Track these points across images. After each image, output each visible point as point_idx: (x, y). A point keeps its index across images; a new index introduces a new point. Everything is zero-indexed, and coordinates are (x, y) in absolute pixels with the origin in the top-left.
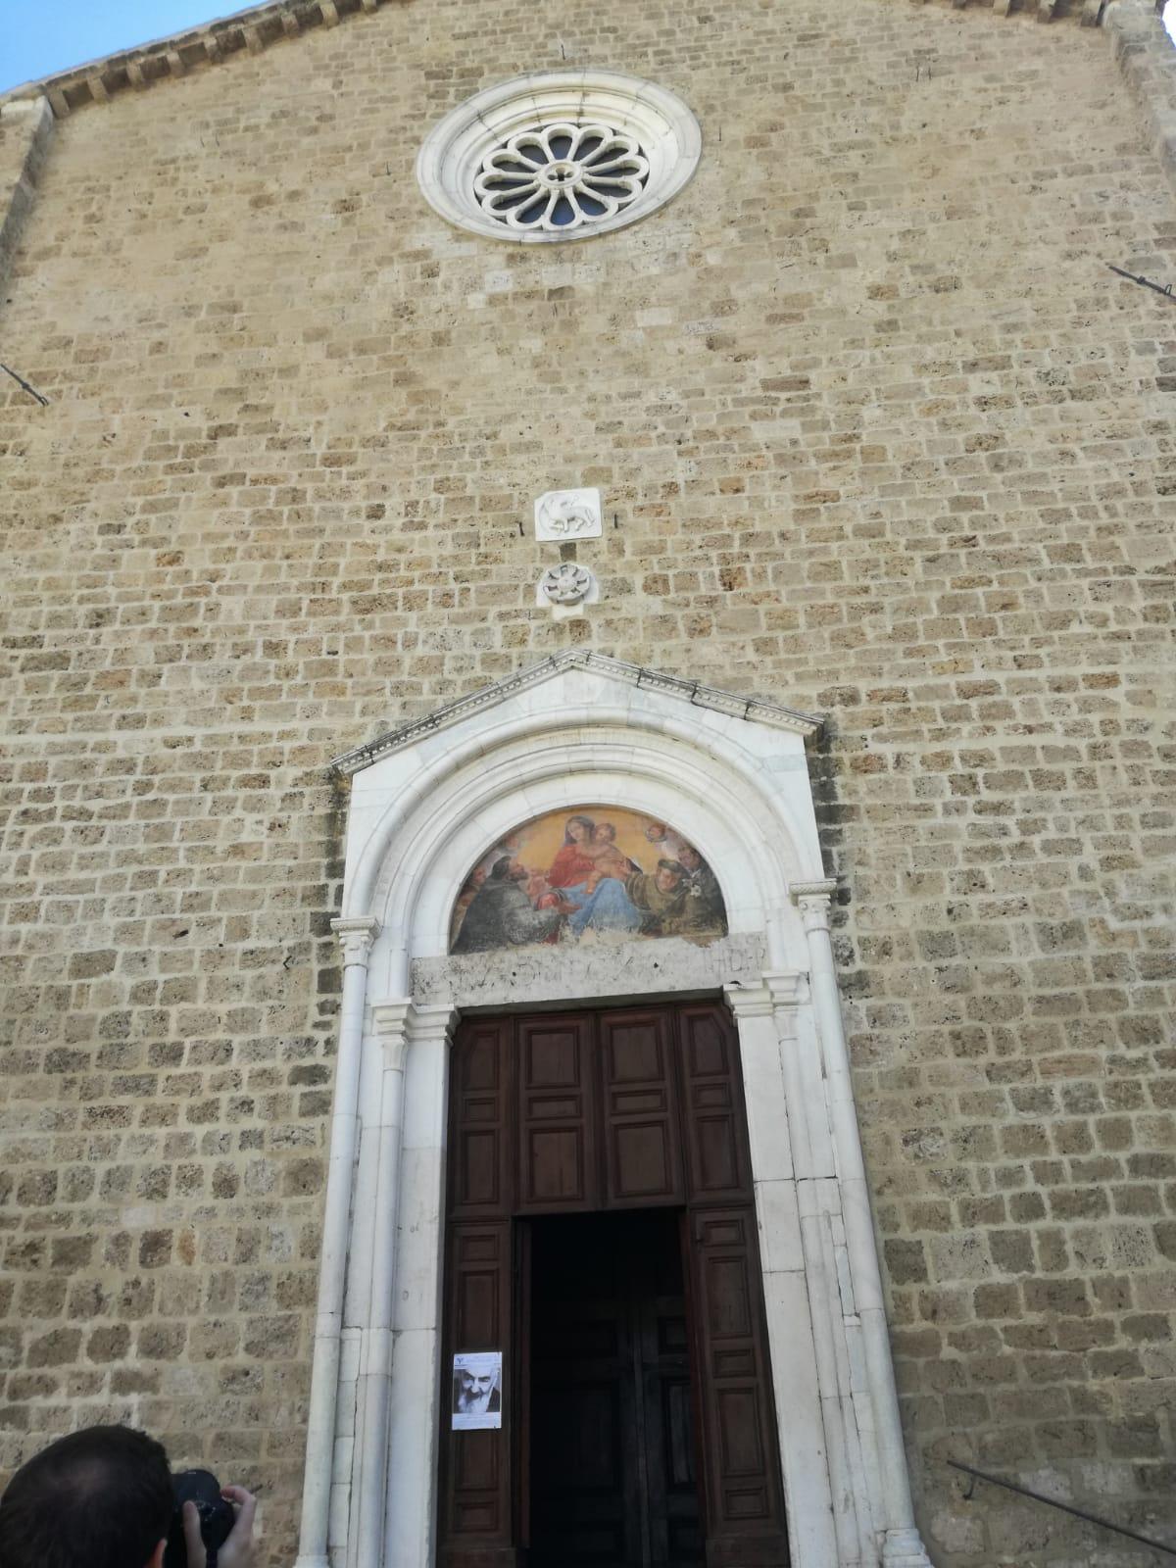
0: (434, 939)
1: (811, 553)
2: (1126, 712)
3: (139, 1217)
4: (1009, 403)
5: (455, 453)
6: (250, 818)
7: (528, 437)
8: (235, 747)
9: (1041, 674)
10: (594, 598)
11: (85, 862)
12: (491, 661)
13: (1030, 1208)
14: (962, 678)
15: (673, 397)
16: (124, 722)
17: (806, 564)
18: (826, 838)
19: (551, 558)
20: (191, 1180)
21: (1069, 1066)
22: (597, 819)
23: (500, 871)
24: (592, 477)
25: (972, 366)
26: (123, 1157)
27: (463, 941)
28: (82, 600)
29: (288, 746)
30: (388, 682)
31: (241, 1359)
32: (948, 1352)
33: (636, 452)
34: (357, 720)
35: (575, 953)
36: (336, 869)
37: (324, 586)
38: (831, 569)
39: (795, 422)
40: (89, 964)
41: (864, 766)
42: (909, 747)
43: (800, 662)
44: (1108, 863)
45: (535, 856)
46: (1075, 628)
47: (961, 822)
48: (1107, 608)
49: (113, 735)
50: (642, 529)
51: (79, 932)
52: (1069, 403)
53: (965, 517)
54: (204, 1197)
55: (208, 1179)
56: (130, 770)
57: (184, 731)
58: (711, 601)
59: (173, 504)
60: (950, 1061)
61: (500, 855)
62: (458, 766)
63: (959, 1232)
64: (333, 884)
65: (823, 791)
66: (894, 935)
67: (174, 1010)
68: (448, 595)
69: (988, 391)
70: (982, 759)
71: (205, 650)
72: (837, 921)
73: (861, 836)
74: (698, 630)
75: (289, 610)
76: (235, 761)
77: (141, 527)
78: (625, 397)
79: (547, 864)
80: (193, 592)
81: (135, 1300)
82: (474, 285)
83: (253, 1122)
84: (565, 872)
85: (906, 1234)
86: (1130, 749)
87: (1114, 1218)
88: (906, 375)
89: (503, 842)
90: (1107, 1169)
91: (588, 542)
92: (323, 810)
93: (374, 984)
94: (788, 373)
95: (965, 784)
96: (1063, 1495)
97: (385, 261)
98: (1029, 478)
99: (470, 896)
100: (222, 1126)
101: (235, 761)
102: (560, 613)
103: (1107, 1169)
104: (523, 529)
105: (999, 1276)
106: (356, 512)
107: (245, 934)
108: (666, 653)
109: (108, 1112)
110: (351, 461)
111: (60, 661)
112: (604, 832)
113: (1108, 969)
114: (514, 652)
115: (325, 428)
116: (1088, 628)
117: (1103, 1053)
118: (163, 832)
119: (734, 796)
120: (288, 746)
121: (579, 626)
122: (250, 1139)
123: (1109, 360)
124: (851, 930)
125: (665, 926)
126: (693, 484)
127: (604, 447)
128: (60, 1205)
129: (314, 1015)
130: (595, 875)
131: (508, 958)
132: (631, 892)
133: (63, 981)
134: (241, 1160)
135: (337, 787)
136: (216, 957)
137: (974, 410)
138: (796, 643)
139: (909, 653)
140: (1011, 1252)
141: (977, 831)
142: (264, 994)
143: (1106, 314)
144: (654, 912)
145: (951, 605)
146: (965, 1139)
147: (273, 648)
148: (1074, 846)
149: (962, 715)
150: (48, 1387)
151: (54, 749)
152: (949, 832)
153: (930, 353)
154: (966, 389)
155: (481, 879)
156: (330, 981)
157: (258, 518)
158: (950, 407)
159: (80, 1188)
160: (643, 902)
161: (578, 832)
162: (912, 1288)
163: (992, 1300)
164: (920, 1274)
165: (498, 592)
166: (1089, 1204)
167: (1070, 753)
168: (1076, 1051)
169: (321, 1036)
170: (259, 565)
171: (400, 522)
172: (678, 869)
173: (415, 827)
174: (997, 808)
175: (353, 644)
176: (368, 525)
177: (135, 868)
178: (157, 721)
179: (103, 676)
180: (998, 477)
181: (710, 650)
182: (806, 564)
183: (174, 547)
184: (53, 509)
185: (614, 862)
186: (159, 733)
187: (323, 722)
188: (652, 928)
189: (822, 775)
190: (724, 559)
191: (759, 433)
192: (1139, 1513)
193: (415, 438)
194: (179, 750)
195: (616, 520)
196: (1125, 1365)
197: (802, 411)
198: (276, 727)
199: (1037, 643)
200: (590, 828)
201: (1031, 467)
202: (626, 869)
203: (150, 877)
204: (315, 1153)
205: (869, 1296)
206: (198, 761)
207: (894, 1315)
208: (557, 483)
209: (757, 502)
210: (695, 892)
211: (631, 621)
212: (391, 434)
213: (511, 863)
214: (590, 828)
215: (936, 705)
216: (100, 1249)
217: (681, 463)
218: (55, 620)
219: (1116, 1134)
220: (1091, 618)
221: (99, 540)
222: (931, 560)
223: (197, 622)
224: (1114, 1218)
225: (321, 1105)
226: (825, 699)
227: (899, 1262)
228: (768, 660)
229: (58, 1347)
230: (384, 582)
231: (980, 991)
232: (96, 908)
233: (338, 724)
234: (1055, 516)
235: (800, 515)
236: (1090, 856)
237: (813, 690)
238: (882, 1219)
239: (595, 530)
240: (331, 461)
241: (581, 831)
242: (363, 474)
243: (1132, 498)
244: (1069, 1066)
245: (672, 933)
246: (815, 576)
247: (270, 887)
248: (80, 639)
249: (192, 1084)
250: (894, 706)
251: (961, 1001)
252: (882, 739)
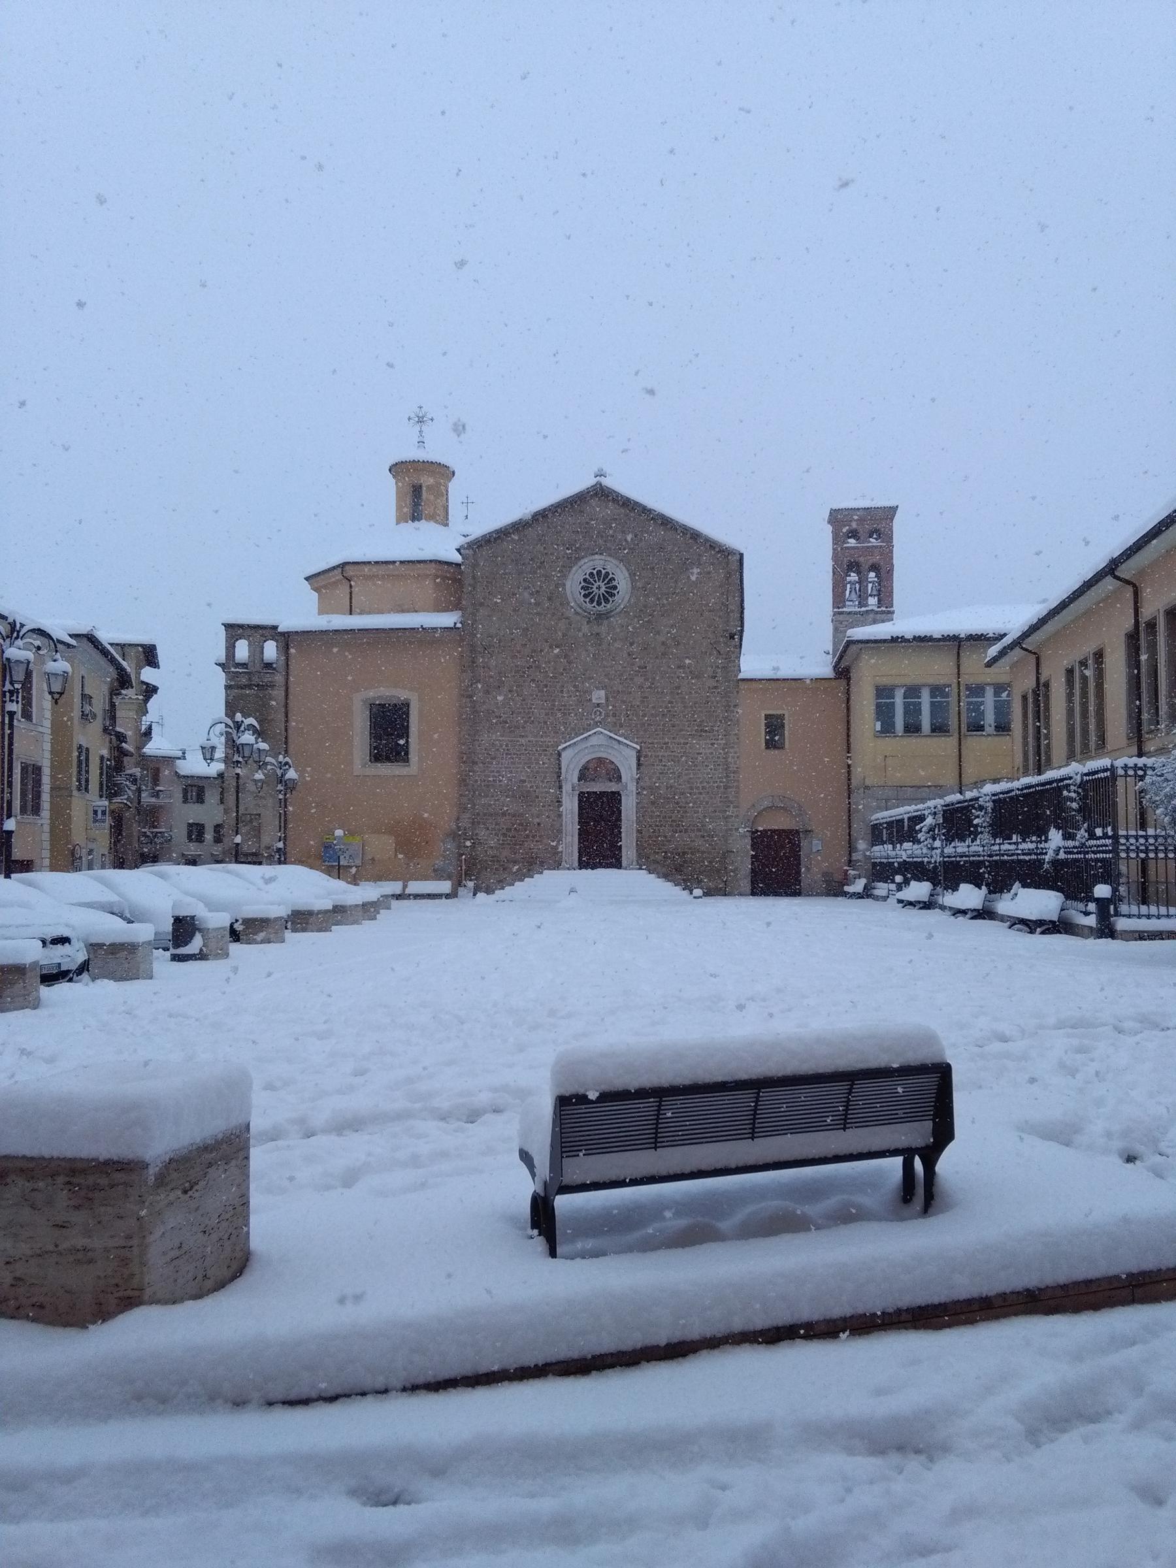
0: (575, 780)
24: (604, 687)
65: (639, 760)
82: (579, 630)
93: (567, 787)
97: (560, 619)
119: (625, 759)
135: (559, 755)
156: (560, 787)
173: (573, 760)
195: (607, 699)
208: (598, 688)
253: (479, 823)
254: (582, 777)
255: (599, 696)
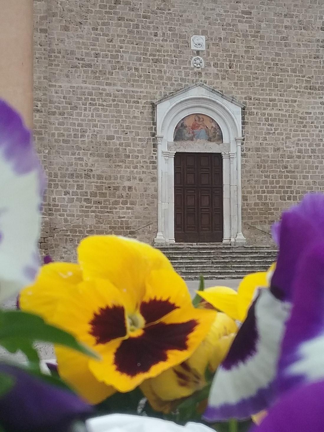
0: (172, 139)
1: (247, 62)
2: (296, 109)
3: (127, 184)
4: (291, 29)
5: (173, 20)
6: (137, 110)
7: (189, 18)
8: (131, 93)
9: (284, 98)
10: (203, 67)
11: (105, 116)
12: (182, 79)
13: (264, 192)
14: (270, 97)
15: (222, 12)
16: (107, 84)
17: (246, 64)
18: (243, 128)
19: (194, 54)
20: (135, 178)
21: (273, 171)
22: (201, 117)
23: (182, 125)
24: (204, 33)
25: (286, 16)
26: (122, 173)
27: (176, 139)
28: (92, 49)
29: (142, 95)
30: (161, 82)
31: (146, 206)
32: (249, 211)
33: (213, 27)
34: (155, 90)
35: (196, 144)
36: (155, 124)
37: (146, 54)
38: (249, 67)
39: (248, 25)
40: (110, 138)
41: (251, 114)
42: (259, 111)
43: (242, 89)
44: (287, 138)
45: (189, 123)
46: (291, 89)
47: (265, 127)
48: (298, 85)
49: (106, 87)
50: (214, 50)
51: (106, 131)
52: (303, 31)
53: (277, 58)
54: (137, 181)
55: (138, 179)
56: (110, 96)
57: (121, 88)
58: (227, 71)
59: (108, 24)
60: (257, 170)
61: (182, 122)
62: (177, 104)
63: (253, 195)
64: (154, 127)
65: (243, 118)
66: (251, 147)
67: (128, 148)
68: (172, 61)
69: (288, 24)
70: (271, 115)
71: (122, 68)
72: (242, 144)
73: (249, 128)
74: (223, 79)
75: (139, 60)
76: (132, 97)
77: (102, 30)
78: (211, 10)
79: (191, 125)
80: (116, 51)
81: (128, 196)
83: (144, 170)
84: (194, 127)
85: (246, 195)
86: (296, 116)
87: (275, 194)
88: (272, 16)
89: (182, 119)
90: (276, 187)
91: (202, 51)
92: (150, 111)
93: (162, 147)
94: (247, 9)
95: (267, 120)
96: (261, 229)
98: (291, 50)
99: (177, 130)
100: (139, 170)
101: (132, 97)
102: (196, 70)
103: (276, 187)
104: (189, 46)
105: (257, 201)
106: (151, 34)
107: (139, 135)
108: (217, 83)
109: (118, 166)
110: (149, 18)
111: (90, 66)
112: (201, 119)
113: (283, 156)
114: (187, 78)
115: (142, 6)
116: (294, 89)
117: (279, 170)
118: (119, 112)
120: (142, 95)
121: (200, 73)
122: (143, 172)
123: (313, 20)
124: (244, 146)
125: (212, 140)
126: (225, 39)
127: (206, 25)
128: (112, 181)
129: (153, 152)
130: (200, 128)
131: (185, 143)
132: (206, 132)
133: (106, 141)
134: (143, 176)
135: (154, 106)
136: (134, 139)
137: (283, 29)
138: (242, 84)
139: (262, 90)
140: (260, 198)
141: (268, 129)
142: (143, 147)
143: (315, 6)
144: (210, 137)
145: (271, 80)
146: (256, 181)
147: (136, 69)
148: (282, 134)
149: (268, 105)
150: (116, 208)
151: (93, 89)
152: (263, 129)
153: (278, 10)
154: (283, 23)
155: (179, 127)
156: (155, 146)
157: (130, 32)
158: (279, 27)
159: (116, 178)
160: (208, 135)
161: (197, 119)
162: (245, 202)
163: (256, 204)
164: (247, 200)
165: (183, 61)
166: (272, 192)
167: (285, 116)
168: (275, 169)
169: (154, 156)
170: (131, 46)
171: (161, 38)
172: (215, 128)
174: (271, 125)
175: (153, 71)
176: (154, 38)
177: (115, 119)
178: (114, 85)
179: (100, 71)
180: (285, 48)
181: (225, 83)
182: (246, 64)
183: (110, 37)
184: (79, 20)
185: (203, 126)
186: (115, 88)
187: (148, 90)
188: (210, 140)
189: (243, 113)
190: (230, 61)
191: (240, 26)
192: (269, 232)
193: (164, 13)
194: (120, 93)
195: (208, 46)
196: (272, 214)
197: (250, 22)
198: (139, 90)
199: (285, 91)
200: (199, 118)
201: (292, 47)
202: (206, 128)
203: (118, 121)
204: (155, 176)
205: (240, 203)
206: (124, 96)
207: (243, 205)
208: (196, 33)
209: (237, 46)
210: (218, 134)
211: (210, 74)
212: (158, 11)
213: (184, 124)
214: (199, 118)
215: (265, 102)
216: (121, 188)
217: (223, 32)
218: (87, 54)
219: (278, 182)
220: (295, 86)
221: (93, 32)
222: (269, 68)
223: (119, 60)
224: (275, 194)
225: (155, 168)
226: (245, 98)
227: (244, 198)
228: (236, 87)
229: (116, 203)
230: (159, 55)
231: (263, 158)
232: (109, 126)
233: (152, 91)
234: (294, 61)
235: (246, 52)
236: (284, 136)
237: (244, 96)
238: (243, 192)
239: (204, 48)
240: (145, 17)
241: (197, 118)
242: (153, 23)
243: (308, 59)
244: (273, 171)
245: (214, 141)
246: (247, 68)
247: (142, 126)
248: (93, 60)
249: (132, 162)
250: (257, 101)
251: (259, 159)
252: (254, 108)
253: (56, 186)
254: (179, 136)
255: (198, 42)
